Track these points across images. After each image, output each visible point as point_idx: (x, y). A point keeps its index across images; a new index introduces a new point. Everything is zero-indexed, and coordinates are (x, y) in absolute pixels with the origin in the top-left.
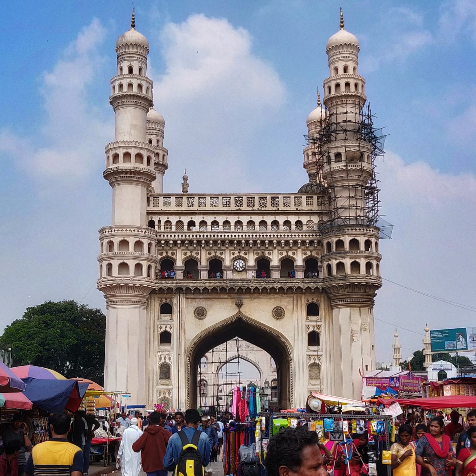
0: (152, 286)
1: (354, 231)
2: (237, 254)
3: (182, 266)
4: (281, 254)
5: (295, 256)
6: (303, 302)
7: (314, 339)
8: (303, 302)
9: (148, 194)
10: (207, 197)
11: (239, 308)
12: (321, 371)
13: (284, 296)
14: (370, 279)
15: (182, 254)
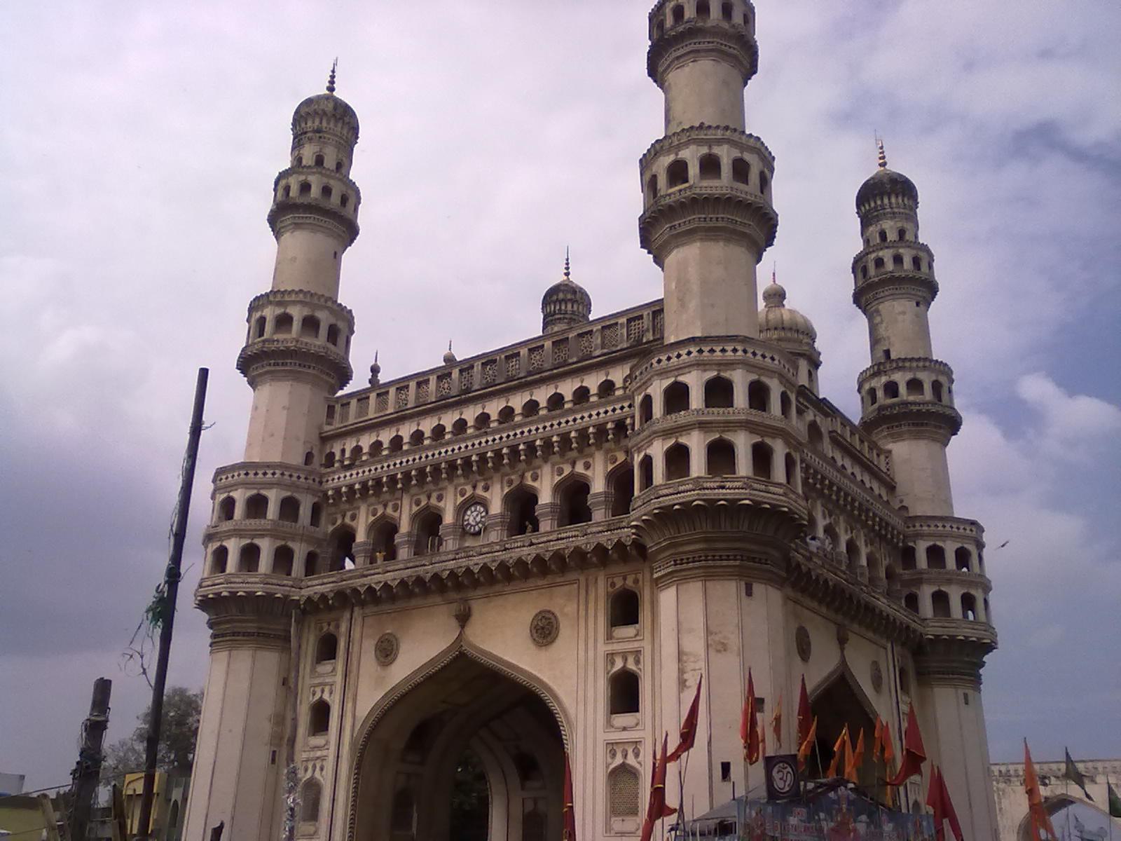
0: (286, 597)
1: (674, 360)
2: (469, 493)
3: (364, 543)
4: (560, 472)
5: (589, 473)
6: (601, 588)
7: (625, 692)
8: (601, 588)
9: (327, 399)
10: (431, 378)
11: (463, 627)
12: (640, 791)
13: (558, 580)
14: (723, 487)
15: (367, 514)
